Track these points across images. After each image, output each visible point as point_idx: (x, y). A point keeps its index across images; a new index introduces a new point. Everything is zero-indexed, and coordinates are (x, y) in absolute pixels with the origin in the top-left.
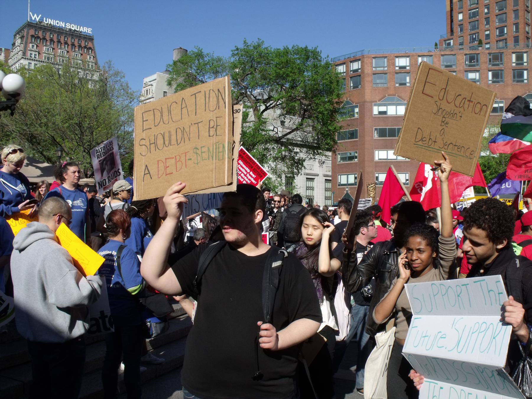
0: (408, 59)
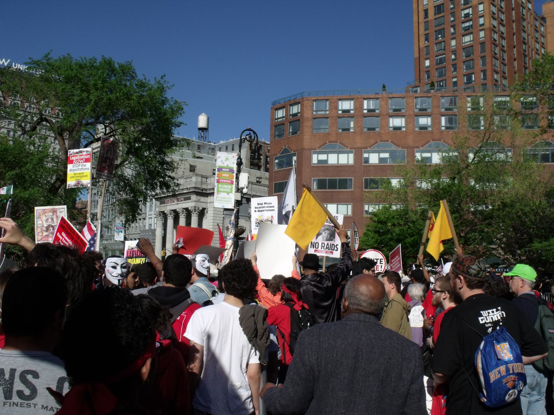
0: (352, 102)
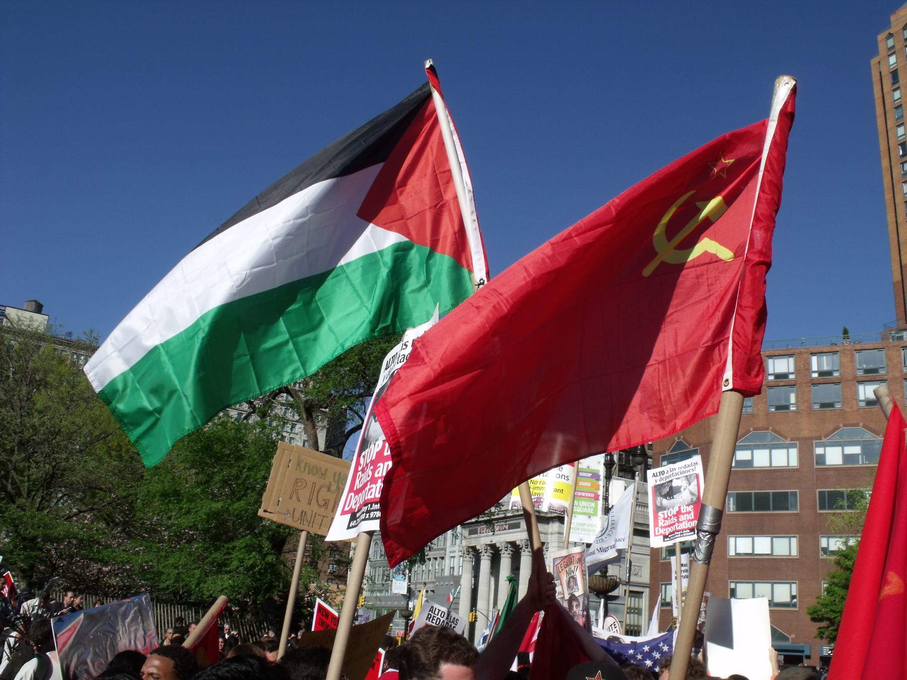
0: (791, 360)
